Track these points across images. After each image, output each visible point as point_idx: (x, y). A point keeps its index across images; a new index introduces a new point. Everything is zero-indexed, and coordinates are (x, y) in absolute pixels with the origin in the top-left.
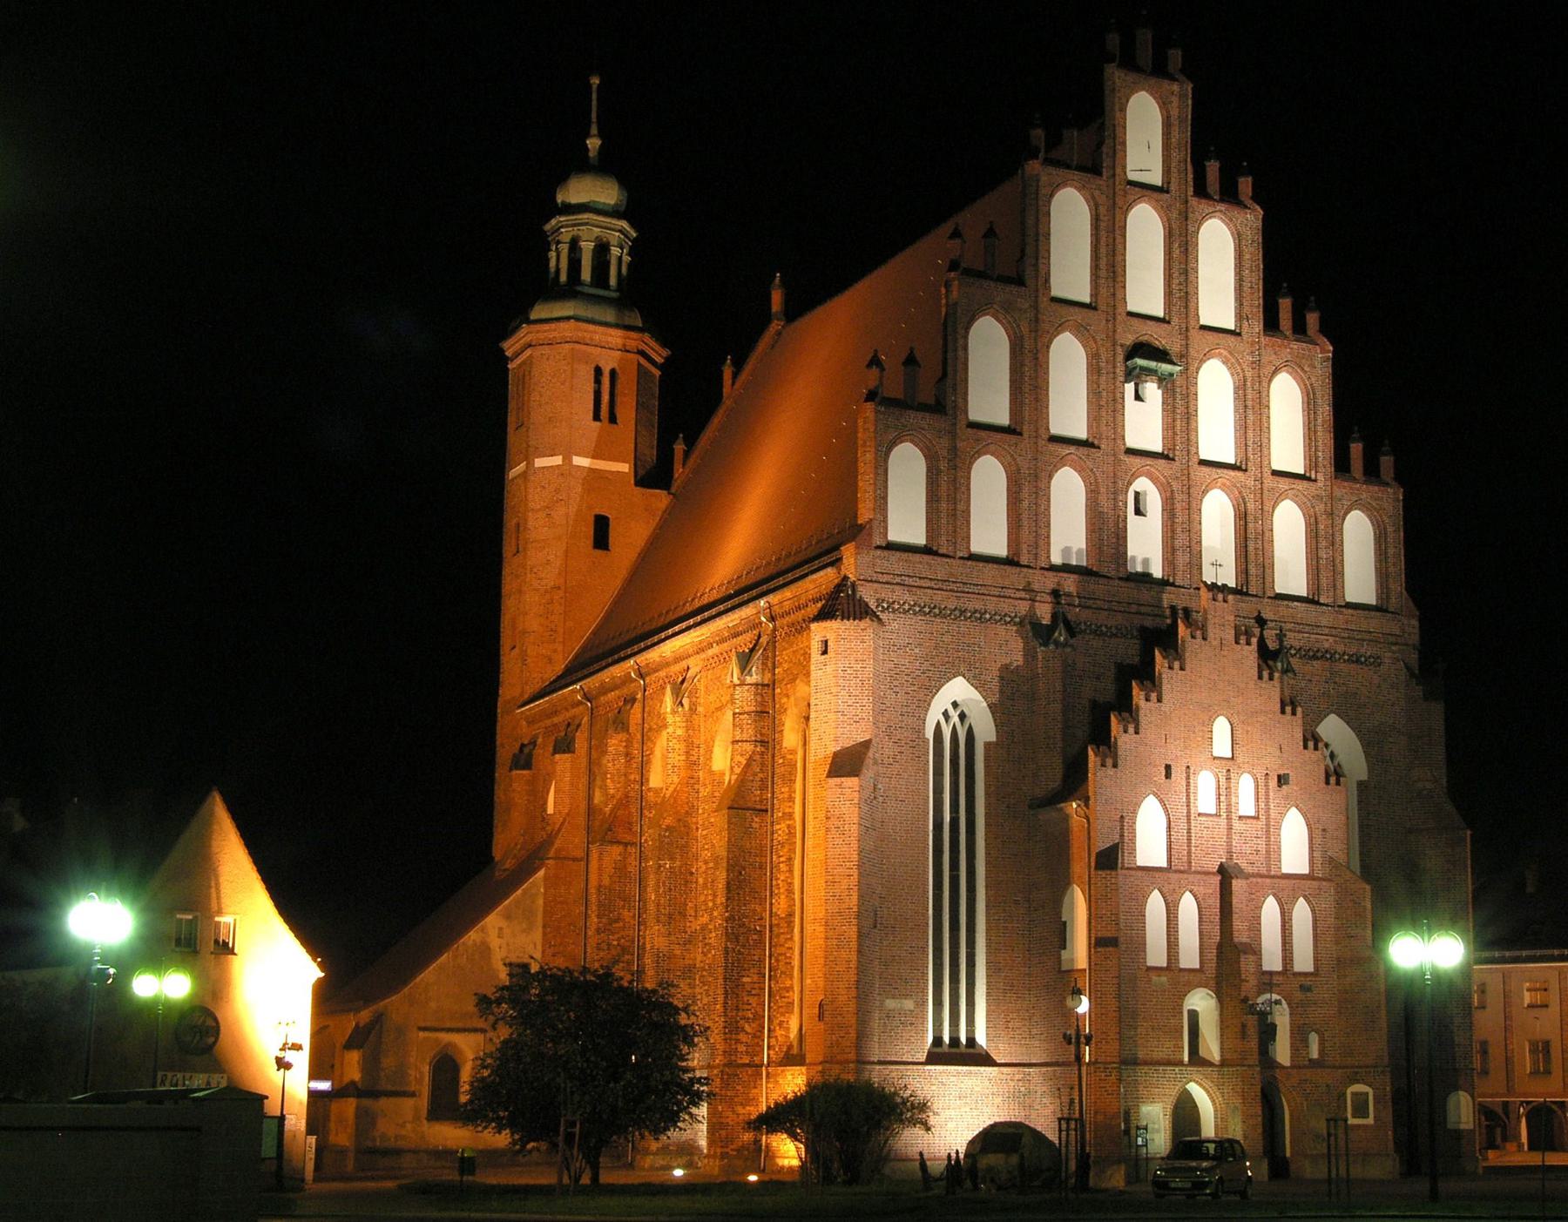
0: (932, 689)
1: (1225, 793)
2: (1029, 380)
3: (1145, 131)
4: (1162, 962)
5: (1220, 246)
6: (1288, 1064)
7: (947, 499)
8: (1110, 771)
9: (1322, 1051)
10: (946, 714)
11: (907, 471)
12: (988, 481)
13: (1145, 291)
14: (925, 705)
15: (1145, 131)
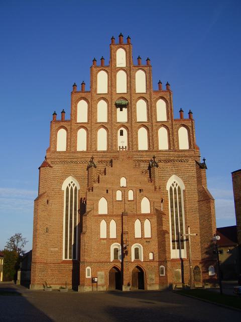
0: (63, 179)
1: (124, 195)
2: (92, 112)
3: (121, 57)
4: (105, 237)
5: (140, 77)
6: (142, 261)
7: (71, 141)
8: (91, 192)
9: (154, 258)
10: (70, 185)
11: (62, 135)
12: (82, 134)
13: (121, 87)
14: (62, 183)
15: (121, 57)
